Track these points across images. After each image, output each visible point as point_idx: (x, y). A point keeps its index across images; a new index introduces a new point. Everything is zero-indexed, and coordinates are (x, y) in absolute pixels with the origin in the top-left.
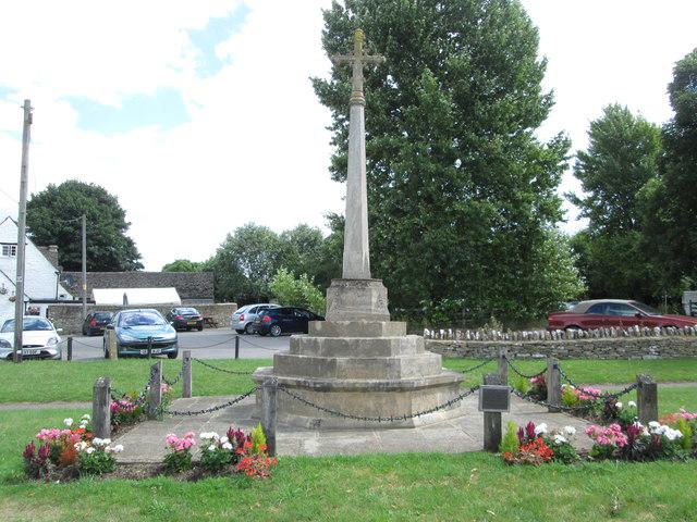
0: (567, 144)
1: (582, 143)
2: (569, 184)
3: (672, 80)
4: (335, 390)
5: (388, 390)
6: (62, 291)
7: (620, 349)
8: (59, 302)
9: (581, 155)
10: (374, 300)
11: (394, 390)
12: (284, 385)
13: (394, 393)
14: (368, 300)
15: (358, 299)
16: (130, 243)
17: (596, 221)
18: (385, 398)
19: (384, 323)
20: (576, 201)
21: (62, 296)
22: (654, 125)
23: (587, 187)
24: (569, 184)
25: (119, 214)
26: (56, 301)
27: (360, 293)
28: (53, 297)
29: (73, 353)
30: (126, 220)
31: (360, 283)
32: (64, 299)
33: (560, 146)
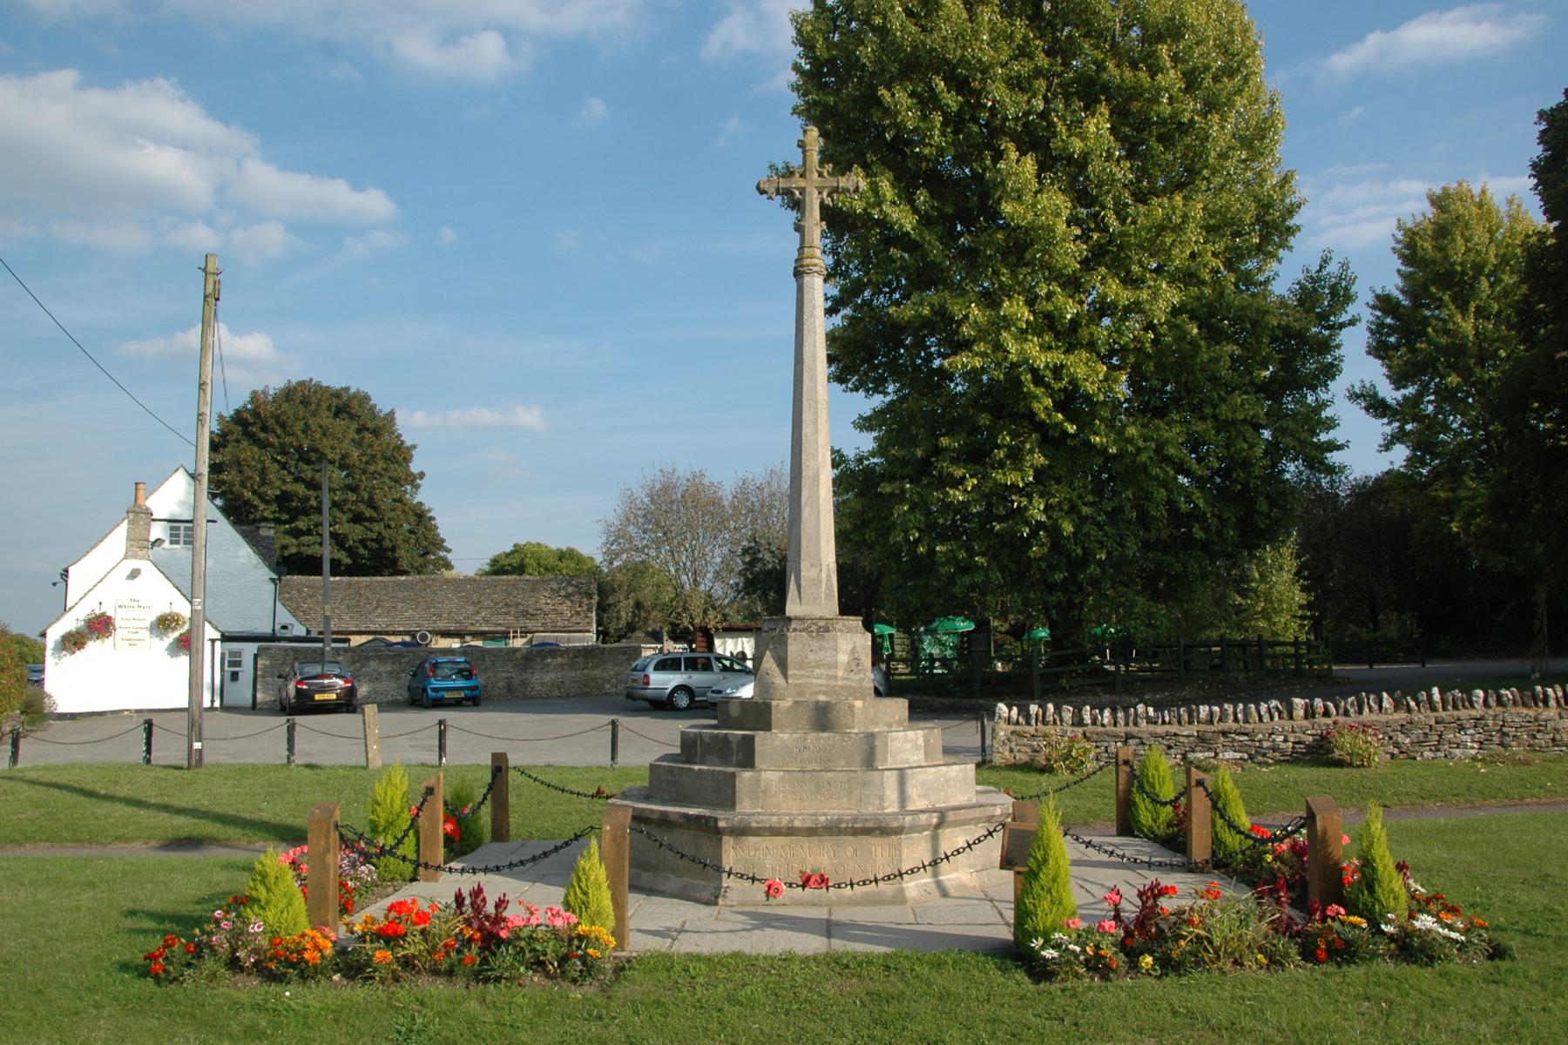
0: (1341, 295)
1: (1380, 275)
2: (1358, 364)
3: (1537, 151)
4: (757, 832)
5: (856, 832)
6: (284, 616)
7: (1400, 738)
8: (280, 639)
9: (1384, 303)
10: (843, 658)
11: (867, 831)
12: (664, 822)
13: (864, 839)
14: (836, 654)
15: (812, 657)
16: (421, 517)
17: (1423, 445)
18: (849, 845)
19: (859, 704)
20: (1377, 407)
21: (285, 627)
22: (1338, 346)
23: (1398, 381)
24: (1358, 364)
25: (399, 455)
26: (273, 638)
27: (815, 644)
28: (266, 629)
29: (297, 747)
30: (414, 468)
31: (821, 629)
32: (288, 634)
33: (1324, 297)
